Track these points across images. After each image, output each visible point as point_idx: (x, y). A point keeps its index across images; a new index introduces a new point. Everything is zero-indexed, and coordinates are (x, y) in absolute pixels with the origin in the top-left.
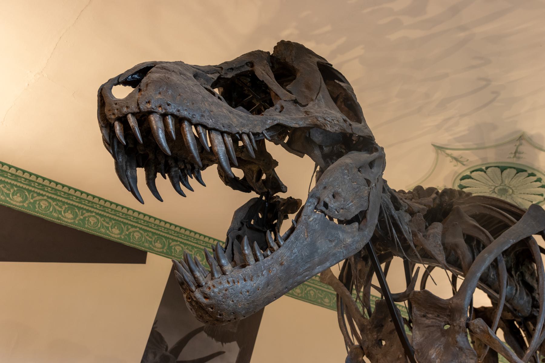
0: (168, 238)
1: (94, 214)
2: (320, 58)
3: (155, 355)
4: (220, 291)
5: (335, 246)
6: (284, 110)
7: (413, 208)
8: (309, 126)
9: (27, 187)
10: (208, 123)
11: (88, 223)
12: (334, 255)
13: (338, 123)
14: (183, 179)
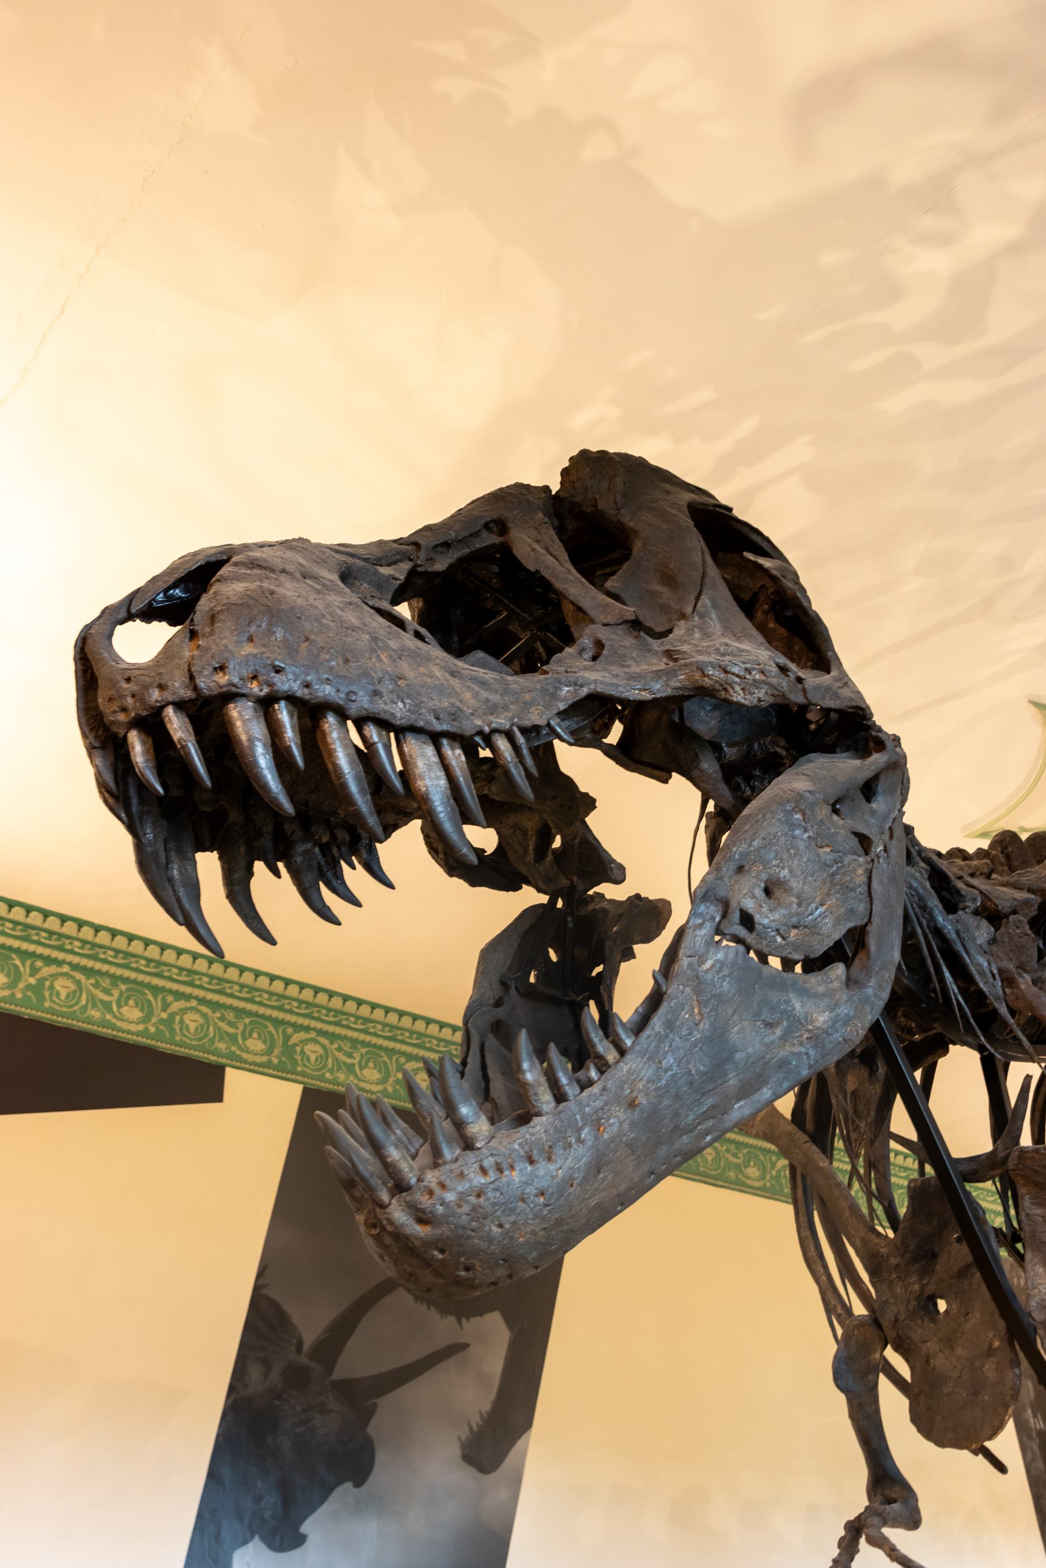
0: (283, 1022)
1: (66, 969)
2: (693, 492)
3: (267, 1365)
4: (462, 1197)
5: (783, 1038)
6: (605, 652)
7: (997, 901)
8: (681, 693)
10: (392, 714)
11: (51, 995)
12: (783, 1063)
13: (763, 677)
14: (330, 875)
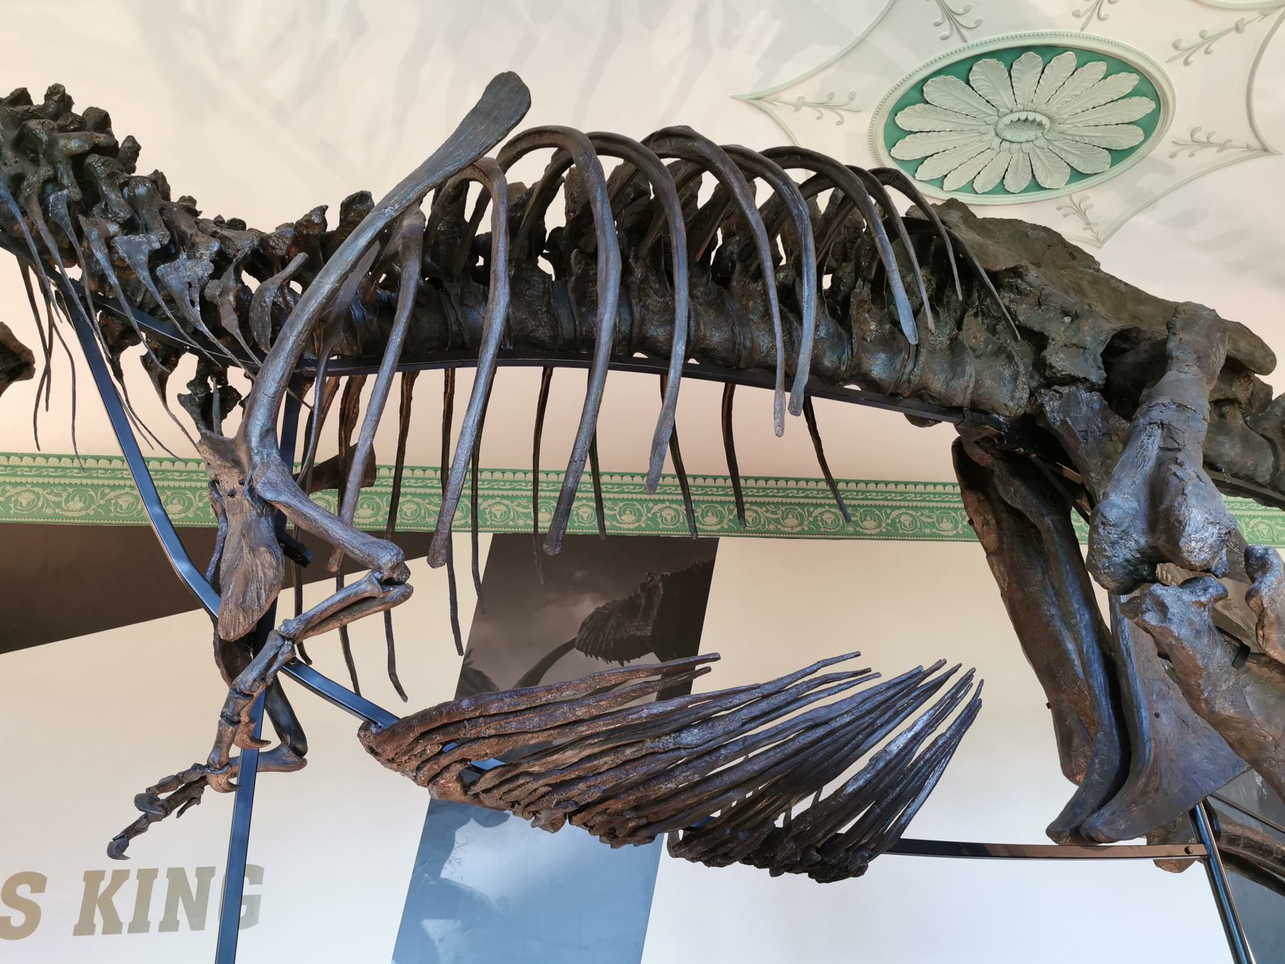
9: (188, 484)
